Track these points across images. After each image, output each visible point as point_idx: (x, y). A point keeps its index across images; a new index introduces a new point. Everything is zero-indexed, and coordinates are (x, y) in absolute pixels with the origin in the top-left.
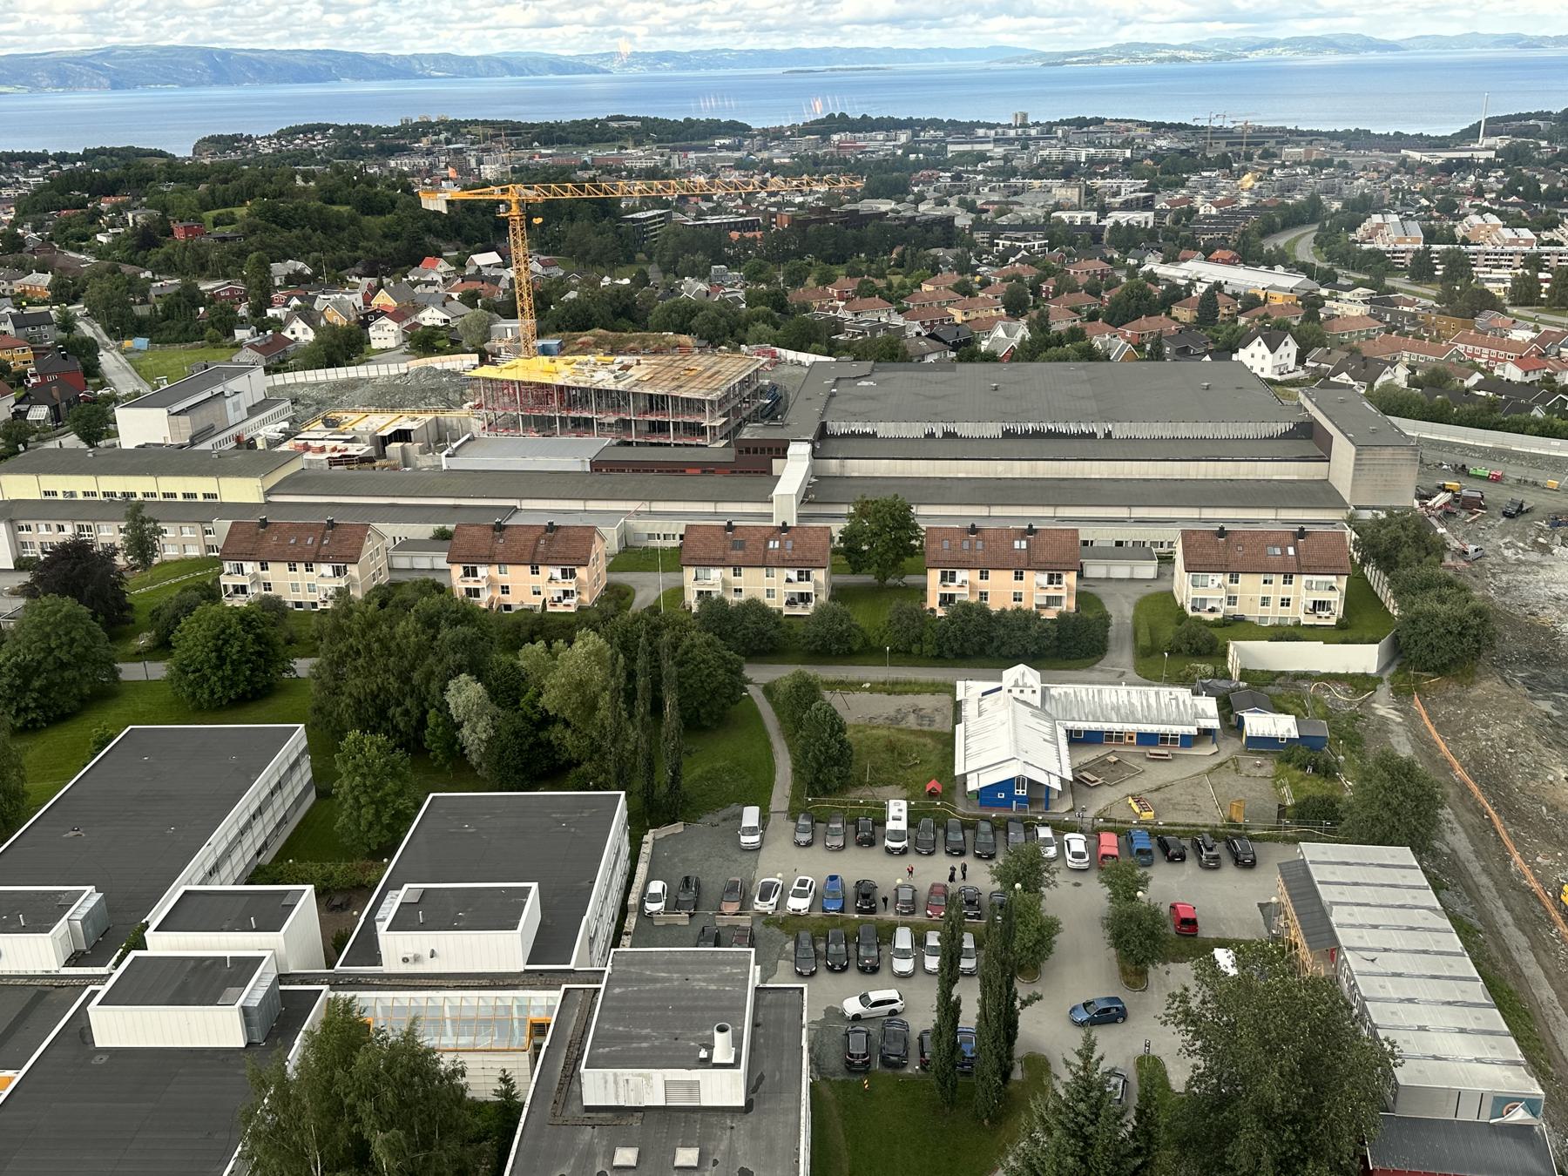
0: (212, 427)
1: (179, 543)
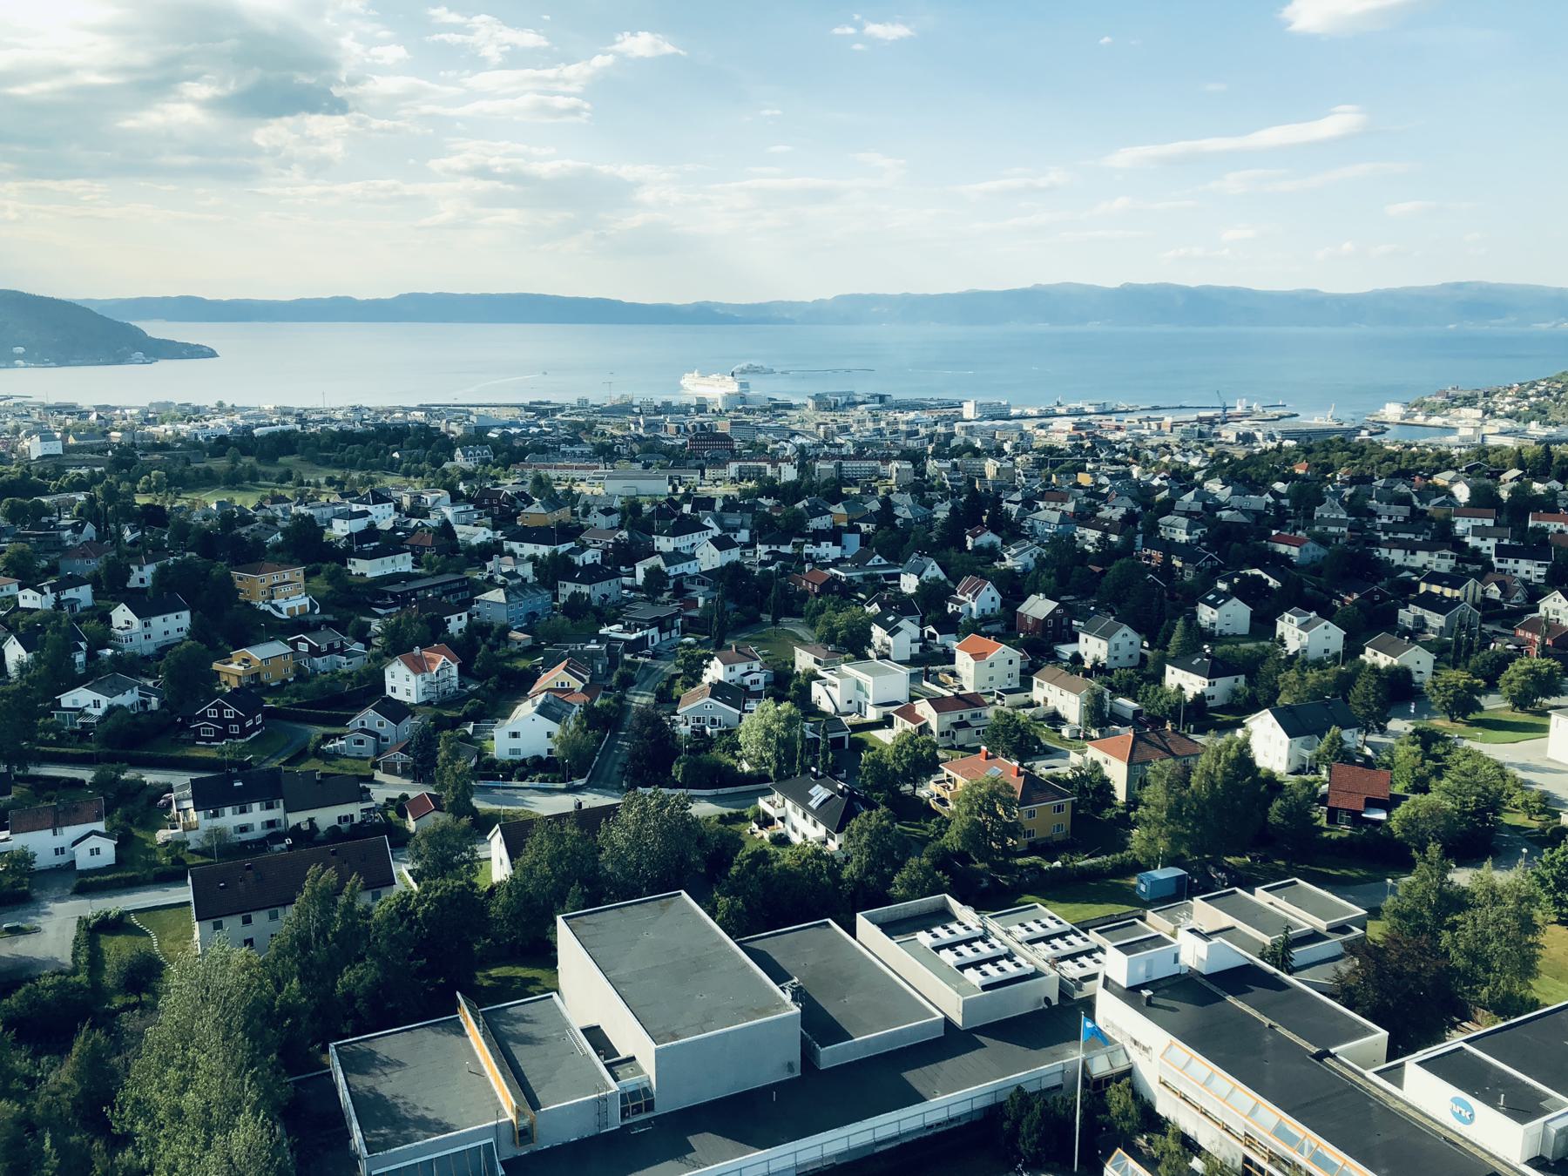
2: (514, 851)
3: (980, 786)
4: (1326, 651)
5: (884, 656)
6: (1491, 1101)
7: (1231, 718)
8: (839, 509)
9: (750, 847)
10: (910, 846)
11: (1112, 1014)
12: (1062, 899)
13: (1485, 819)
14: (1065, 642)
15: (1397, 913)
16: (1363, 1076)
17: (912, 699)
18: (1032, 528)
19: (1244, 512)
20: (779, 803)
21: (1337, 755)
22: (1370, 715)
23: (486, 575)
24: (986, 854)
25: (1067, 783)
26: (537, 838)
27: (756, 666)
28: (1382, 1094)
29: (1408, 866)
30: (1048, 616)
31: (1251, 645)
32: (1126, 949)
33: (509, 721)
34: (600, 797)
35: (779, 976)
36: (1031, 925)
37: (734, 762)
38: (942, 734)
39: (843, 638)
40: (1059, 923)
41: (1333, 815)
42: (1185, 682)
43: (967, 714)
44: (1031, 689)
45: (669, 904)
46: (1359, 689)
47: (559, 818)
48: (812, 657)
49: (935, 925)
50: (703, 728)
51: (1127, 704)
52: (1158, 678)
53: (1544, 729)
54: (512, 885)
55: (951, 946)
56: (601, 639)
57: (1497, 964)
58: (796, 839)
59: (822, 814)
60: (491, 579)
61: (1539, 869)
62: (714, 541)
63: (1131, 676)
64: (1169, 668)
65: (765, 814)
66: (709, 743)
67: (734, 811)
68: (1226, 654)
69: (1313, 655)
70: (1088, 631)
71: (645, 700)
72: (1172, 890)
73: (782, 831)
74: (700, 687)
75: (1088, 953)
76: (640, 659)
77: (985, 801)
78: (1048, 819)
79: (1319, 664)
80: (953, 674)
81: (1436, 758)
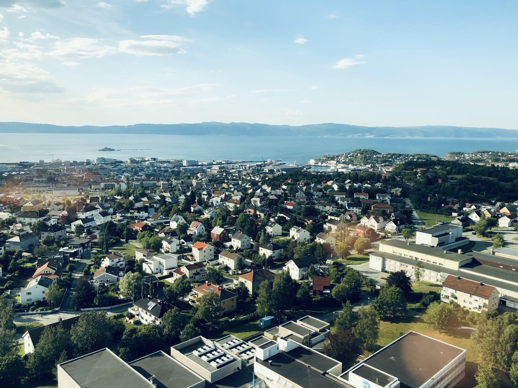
0: (444, 243)
1: (430, 277)
2: (35, 341)
3: (208, 296)
4: (305, 239)
5: (167, 252)
6: (374, 381)
7: (280, 263)
8: (145, 199)
9: (128, 328)
10: (185, 320)
11: (260, 370)
12: (237, 332)
13: (357, 290)
14: (227, 242)
15: (339, 323)
16: (337, 379)
17: (179, 266)
18: (212, 203)
19: (276, 195)
20: (136, 309)
21: (313, 273)
22: (321, 259)
23: (10, 231)
24: (210, 319)
25: (234, 291)
26: (46, 335)
27: (122, 259)
28: (343, 383)
29: (341, 308)
30: (221, 234)
31: (283, 238)
32: (262, 347)
33: (26, 289)
34: (66, 314)
35: (147, 375)
36: (230, 343)
37: (117, 295)
38: (190, 278)
39: (153, 246)
40: (239, 341)
41: (314, 294)
42: (265, 252)
43: (198, 270)
44: (218, 259)
45: (101, 354)
46: (317, 252)
47: (54, 325)
48: (142, 254)
49: (199, 348)
50: (104, 284)
51: (249, 261)
52: (257, 252)
53: (368, 259)
54: (36, 354)
55: (205, 354)
56: (60, 253)
57: (368, 336)
58: (143, 322)
59: (153, 312)
60: (12, 233)
61: (374, 304)
62: (101, 213)
63: (249, 252)
64: (260, 248)
65: (131, 314)
66: (107, 290)
67: (119, 314)
68: (278, 242)
69: (302, 240)
70: (235, 237)
71: (80, 275)
72: (270, 323)
73: (138, 319)
74: (101, 269)
75: (249, 350)
76: (76, 260)
77: (210, 301)
78: (229, 304)
79: (303, 244)
80: (192, 256)
81: (341, 271)
